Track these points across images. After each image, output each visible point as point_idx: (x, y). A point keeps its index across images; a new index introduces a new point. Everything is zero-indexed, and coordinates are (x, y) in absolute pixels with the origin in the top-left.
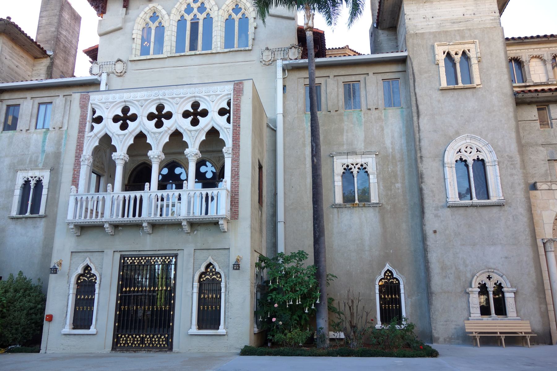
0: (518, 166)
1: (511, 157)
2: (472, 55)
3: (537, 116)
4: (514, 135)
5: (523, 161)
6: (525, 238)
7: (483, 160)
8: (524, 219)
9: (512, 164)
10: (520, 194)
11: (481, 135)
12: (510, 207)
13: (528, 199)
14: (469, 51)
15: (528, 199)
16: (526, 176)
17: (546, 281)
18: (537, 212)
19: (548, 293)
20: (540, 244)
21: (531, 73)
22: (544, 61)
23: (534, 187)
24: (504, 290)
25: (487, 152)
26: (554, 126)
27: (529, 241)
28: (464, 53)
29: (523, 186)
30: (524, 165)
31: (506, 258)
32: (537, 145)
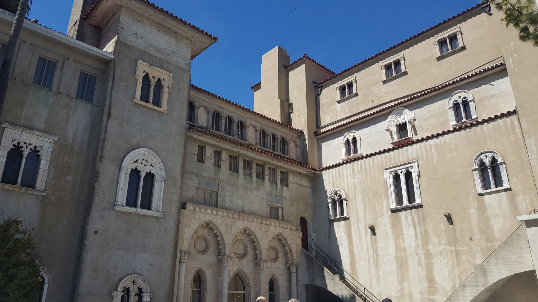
0: (178, 186)
1: (175, 178)
2: (165, 84)
3: (197, 151)
4: (180, 160)
5: (182, 183)
6: (169, 250)
7: (153, 175)
8: (173, 232)
9: (174, 184)
10: (174, 210)
11: (156, 153)
12: (164, 220)
13: (179, 215)
14: (164, 80)
15: (179, 215)
16: (181, 195)
17: (176, 288)
18: (182, 227)
19: (175, 298)
20: (178, 256)
21: (199, 117)
22: (208, 112)
23: (183, 206)
24: (144, 294)
25: (158, 169)
26: (206, 162)
27: (171, 252)
28: (159, 80)
29: (178, 204)
30: (181, 188)
31: (151, 265)
32: (192, 173)
